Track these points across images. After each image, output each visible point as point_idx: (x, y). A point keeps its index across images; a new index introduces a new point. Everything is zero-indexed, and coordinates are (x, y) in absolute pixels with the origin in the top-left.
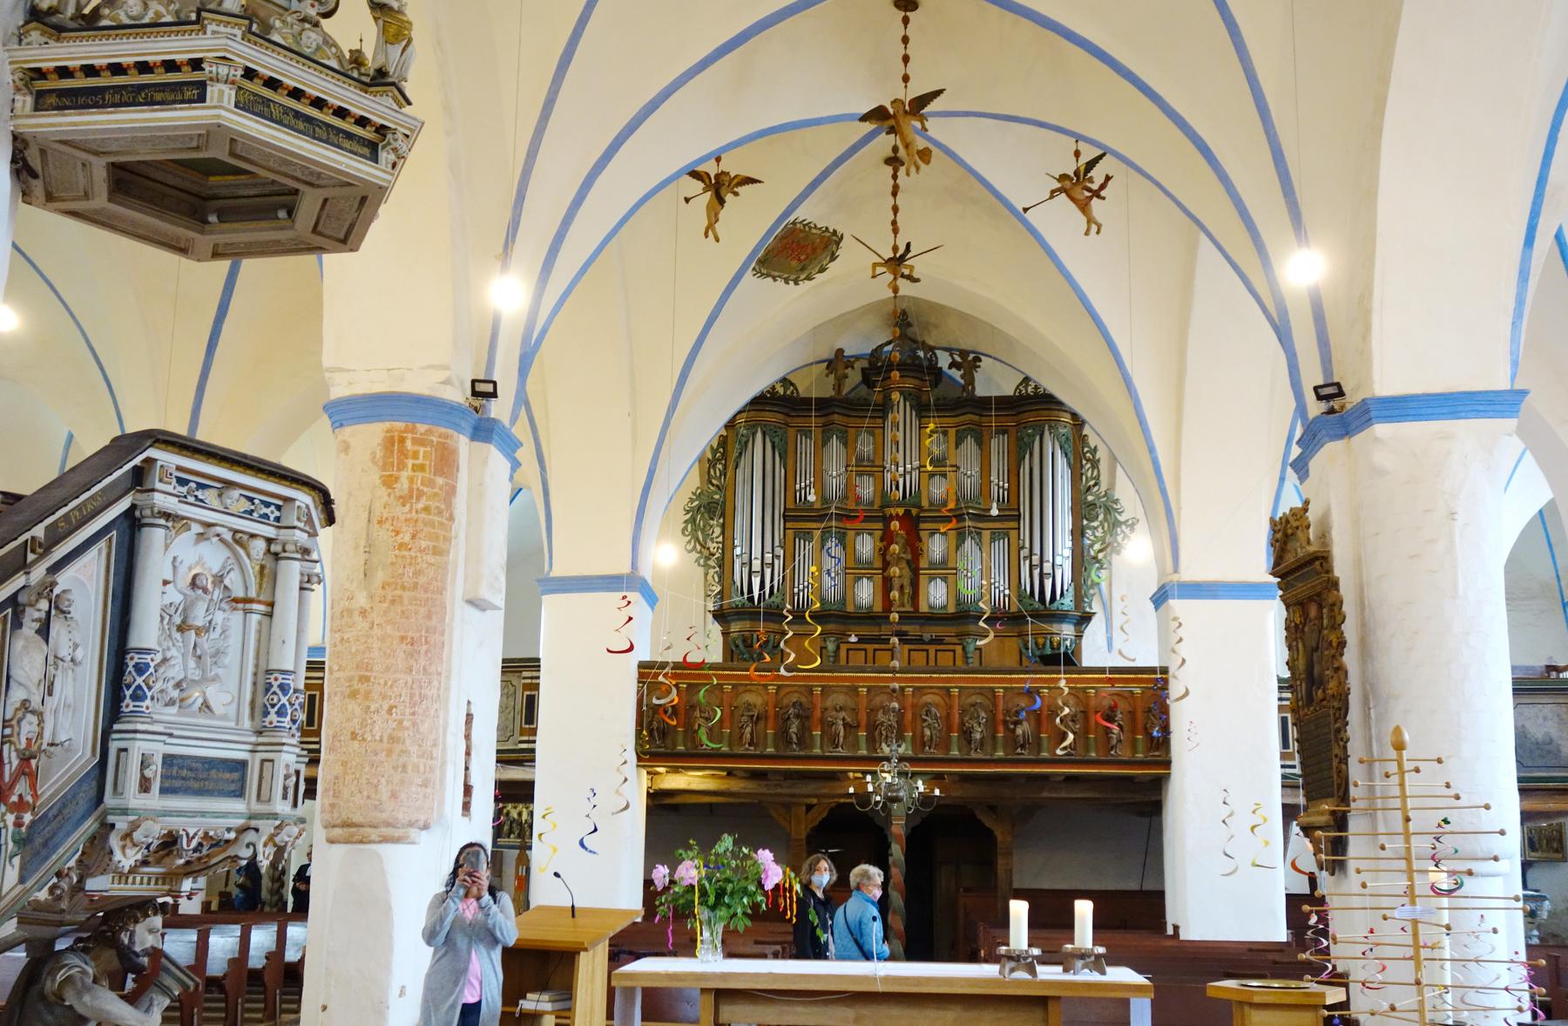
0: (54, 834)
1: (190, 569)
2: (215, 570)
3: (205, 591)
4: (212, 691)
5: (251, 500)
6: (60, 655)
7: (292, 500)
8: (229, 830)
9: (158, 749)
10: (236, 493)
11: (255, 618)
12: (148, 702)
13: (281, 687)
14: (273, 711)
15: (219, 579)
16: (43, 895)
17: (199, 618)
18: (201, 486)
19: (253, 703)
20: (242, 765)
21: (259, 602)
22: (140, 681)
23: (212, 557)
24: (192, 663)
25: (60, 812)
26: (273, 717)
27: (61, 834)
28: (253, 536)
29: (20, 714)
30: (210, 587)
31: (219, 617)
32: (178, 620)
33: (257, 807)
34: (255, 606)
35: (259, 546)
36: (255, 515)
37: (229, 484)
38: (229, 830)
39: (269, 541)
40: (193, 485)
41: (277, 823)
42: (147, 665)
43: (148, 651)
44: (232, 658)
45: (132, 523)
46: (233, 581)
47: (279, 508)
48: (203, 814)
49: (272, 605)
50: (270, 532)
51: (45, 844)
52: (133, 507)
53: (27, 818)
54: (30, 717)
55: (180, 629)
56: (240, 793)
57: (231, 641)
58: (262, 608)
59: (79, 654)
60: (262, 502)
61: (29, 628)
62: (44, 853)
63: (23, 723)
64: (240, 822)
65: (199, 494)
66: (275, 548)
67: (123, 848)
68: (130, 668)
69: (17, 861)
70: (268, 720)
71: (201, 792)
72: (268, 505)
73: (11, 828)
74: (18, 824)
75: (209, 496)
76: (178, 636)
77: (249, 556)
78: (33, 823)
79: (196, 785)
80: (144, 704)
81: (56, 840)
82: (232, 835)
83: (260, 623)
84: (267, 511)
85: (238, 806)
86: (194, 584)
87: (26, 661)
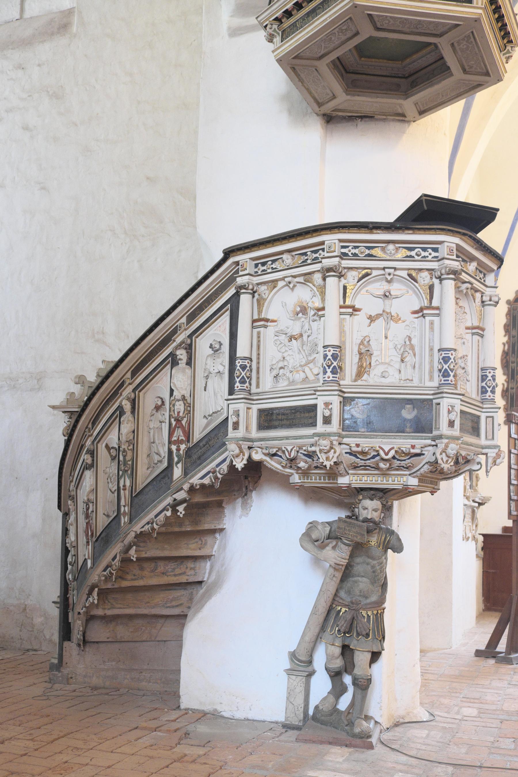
0: (204, 453)
12: (238, 384)
14: (329, 371)
16: (206, 481)
18: (274, 261)
25: (207, 443)
27: (209, 454)
28: (313, 272)
36: (309, 261)
48: (287, 438)
51: (199, 458)
53: (183, 447)
59: (221, 369)
60: (312, 252)
61: (182, 364)
62: (198, 462)
68: (238, 368)
69: (180, 465)
70: (326, 376)
71: (290, 426)
73: (175, 451)
74: (178, 450)
77: (314, 285)
79: (288, 423)
81: (205, 456)
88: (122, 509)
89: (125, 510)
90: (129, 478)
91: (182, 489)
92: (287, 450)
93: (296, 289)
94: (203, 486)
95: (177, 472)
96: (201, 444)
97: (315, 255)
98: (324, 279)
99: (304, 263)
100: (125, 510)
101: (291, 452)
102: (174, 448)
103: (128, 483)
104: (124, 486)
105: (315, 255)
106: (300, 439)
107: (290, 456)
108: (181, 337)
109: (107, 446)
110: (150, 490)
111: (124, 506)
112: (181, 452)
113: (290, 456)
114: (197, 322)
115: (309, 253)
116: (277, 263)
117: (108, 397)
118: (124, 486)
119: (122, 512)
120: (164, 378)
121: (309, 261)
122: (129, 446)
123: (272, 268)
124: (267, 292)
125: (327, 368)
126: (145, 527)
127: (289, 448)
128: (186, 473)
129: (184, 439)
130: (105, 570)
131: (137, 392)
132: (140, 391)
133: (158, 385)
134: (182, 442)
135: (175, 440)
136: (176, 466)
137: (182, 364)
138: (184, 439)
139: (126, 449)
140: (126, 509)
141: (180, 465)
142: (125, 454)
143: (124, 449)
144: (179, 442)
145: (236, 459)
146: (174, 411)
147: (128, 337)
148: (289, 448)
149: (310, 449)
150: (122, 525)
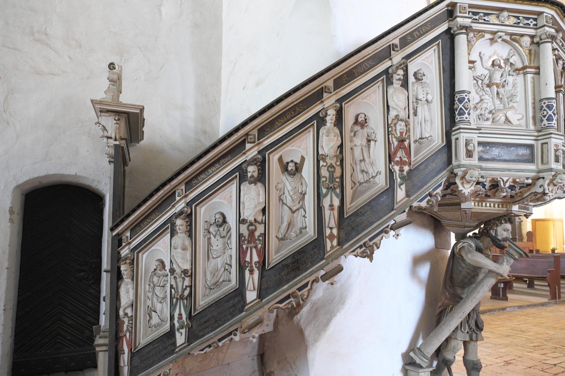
1: (490, 57)
2: (505, 57)
3: (500, 67)
4: (510, 114)
5: (518, 18)
6: (419, 98)
7: (543, 13)
8: (527, 179)
9: (475, 138)
10: (506, 14)
11: (529, 76)
12: (466, 115)
13: (548, 106)
14: (545, 119)
15: (507, 60)
16: (424, 204)
17: (497, 79)
18: (486, 14)
19: (534, 118)
20: (531, 147)
21: (530, 67)
22: (461, 106)
23: (501, 51)
24: (497, 102)
26: (545, 122)
28: (522, 35)
29: (395, 122)
30: (502, 65)
31: (510, 79)
32: (486, 81)
33: (541, 167)
34: (528, 70)
35: (526, 41)
36: (521, 25)
37: (502, 10)
38: (527, 179)
39: (532, 37)
40: (482, 14)
41: (553, 173)
42: (464, 99)
43: (463, 92)
44: (520, 97)
45: (450, 37)
46: (515, 59)
47: (535, 20)
48: (509, 170)
49: (538, 68)
50: (532, 32)
52: (449, 29)
53: (406, 168)
54: (400, 122)
55: (489, 86)
56: (531, 160)
57: (518, 89)
58: (533, 70)
59: (430, 97)
60: (524, 17)
61: (397, 84)
63: (397, 125)
64: (533, 174)
65: (486, 18)
66: (536, 40)
67: (463, 183)
68: (457, 102)
69: (403, 187)
72: (528, 19)
73: (398, 172)
74: (401, 170)
75: (493, 19)
76: (488, 89)
78: (410, 171)
80: (465, 116)
82: (530, 181)
83: (533, 78)
84: (529, 22)
85: (532, 167)
86: (493, 65)
87: (395, 98)
88: (328, 232)
89: (331, 232)
90: (337, 196)
91: (405, 211)
92: (503, 180)
93: (496, 44)
94: (420, 208)
95: (401, 193)
96: (421, 168)
97: (527, 22)
98: (537, 43)
99: (516, 25)
100: (331, 232)
101: (506, 182)
102: (397, 168)
103: (336, 202)
104: (331, 206)
105: (527, 22)
106: (522, 172)
107: (504, 186)
108: (397, 58)
109: (280, 159)
110: (367, 211)
111: (331, 228)
112: (405, 173)
113: (504, 186)
114: (411, 48)
115: (521, 18)
116: (490, 17)
117: (295, 103)
118: (331, 206)
119: (327, 235)
120: (372, 95)
121: (521, 25)
122: (337, 161)
123: (484, 20)
124: (474, 39)
125: (553, 116)
126: (356, 251)
127: (505, 179)
128: (408, 195)
129: (407, 161)
130: (281, 302)
131: (343, 104)
132: (345, 104)
133: (365, 101)
134: (404, 163)
135: (398, 161)
136: (400, 187)
137: (397, 84)
138: (407, 161)
139: (334, 165)
140: (335, 232)
141: (403, 187)
142: (333, 169)
143: (331, 164)
144: (401, 163)
145: (465, 185)
146: (396, 130)
147: (80, 46)
148: (505, 179)
149: (526, 181)
150: (329, 249)
